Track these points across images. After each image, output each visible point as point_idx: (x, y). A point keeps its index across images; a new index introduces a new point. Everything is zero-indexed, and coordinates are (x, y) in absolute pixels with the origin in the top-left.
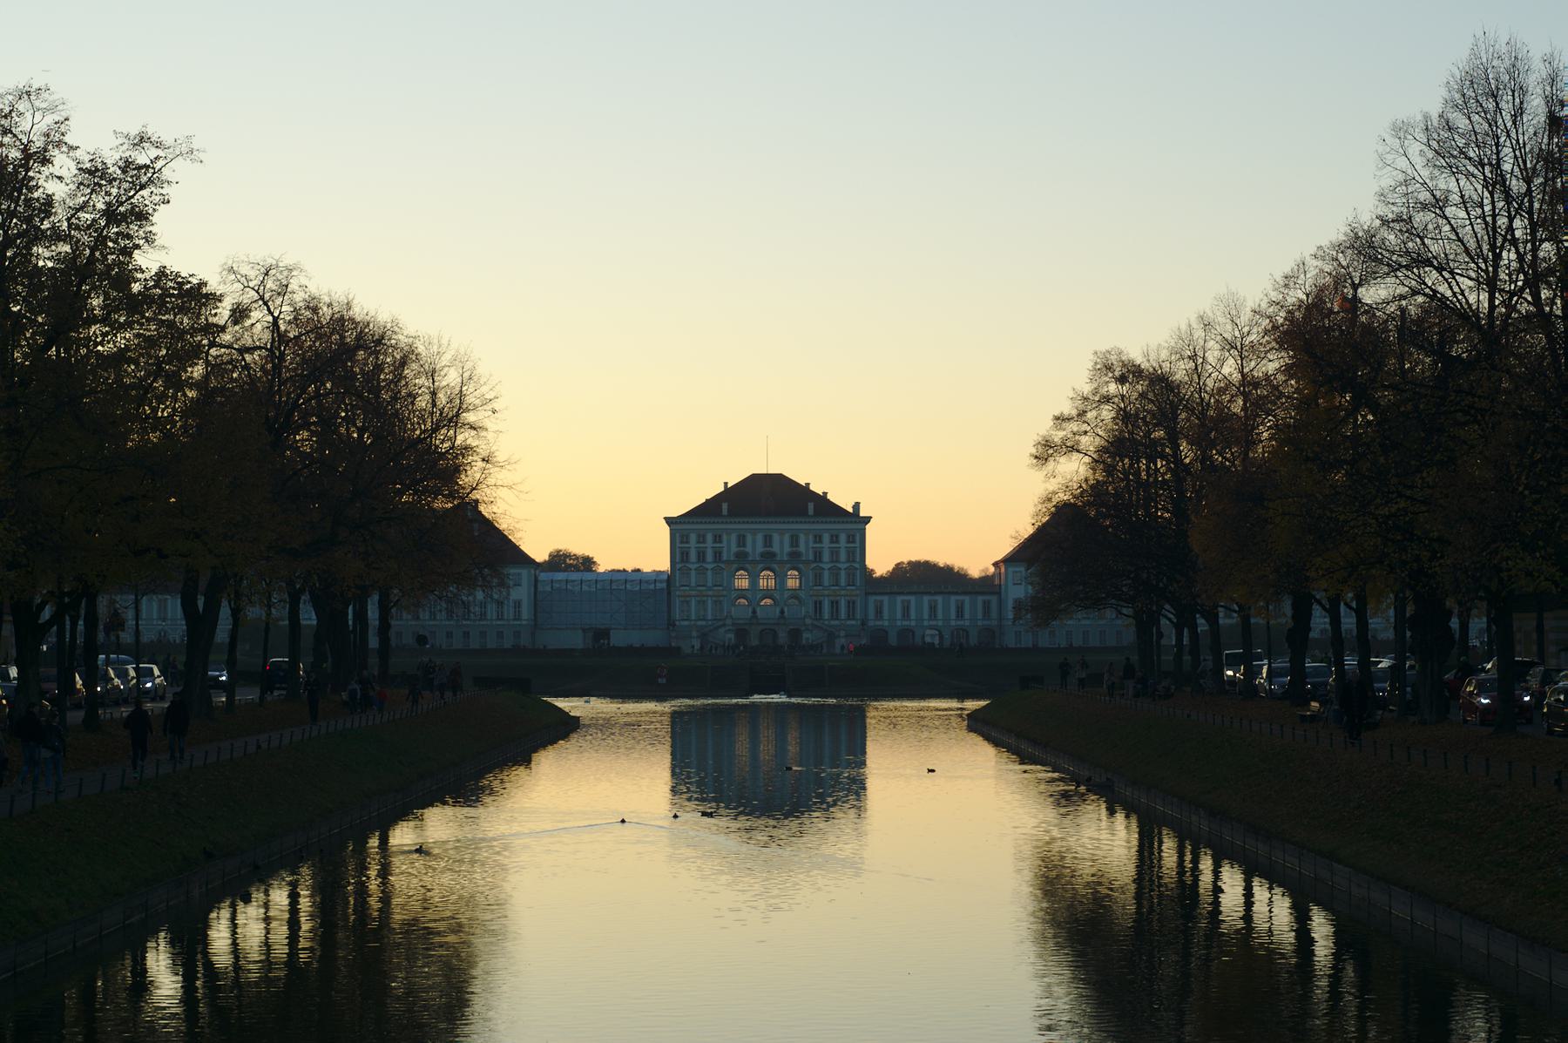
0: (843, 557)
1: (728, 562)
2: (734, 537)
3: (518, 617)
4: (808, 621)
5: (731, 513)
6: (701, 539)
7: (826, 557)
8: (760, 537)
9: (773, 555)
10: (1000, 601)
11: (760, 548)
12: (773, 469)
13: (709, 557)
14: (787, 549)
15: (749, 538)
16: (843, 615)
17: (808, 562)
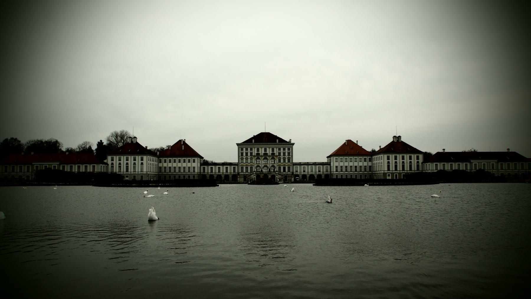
0: (287, 154)
1: (254, 156)
2: (256, 149)
3: (194, 171)
5: (255, 142)
6: (247, 149)
7: (282, 154)
8: (263, 149)
9: (267, 154)
10: (331, 167)
11: (263, 152)
12: (267, 131)
13: (249, 154)
14: (271, 152)
15: (260, 149)
16: (287, 171)
17: (277, 156)
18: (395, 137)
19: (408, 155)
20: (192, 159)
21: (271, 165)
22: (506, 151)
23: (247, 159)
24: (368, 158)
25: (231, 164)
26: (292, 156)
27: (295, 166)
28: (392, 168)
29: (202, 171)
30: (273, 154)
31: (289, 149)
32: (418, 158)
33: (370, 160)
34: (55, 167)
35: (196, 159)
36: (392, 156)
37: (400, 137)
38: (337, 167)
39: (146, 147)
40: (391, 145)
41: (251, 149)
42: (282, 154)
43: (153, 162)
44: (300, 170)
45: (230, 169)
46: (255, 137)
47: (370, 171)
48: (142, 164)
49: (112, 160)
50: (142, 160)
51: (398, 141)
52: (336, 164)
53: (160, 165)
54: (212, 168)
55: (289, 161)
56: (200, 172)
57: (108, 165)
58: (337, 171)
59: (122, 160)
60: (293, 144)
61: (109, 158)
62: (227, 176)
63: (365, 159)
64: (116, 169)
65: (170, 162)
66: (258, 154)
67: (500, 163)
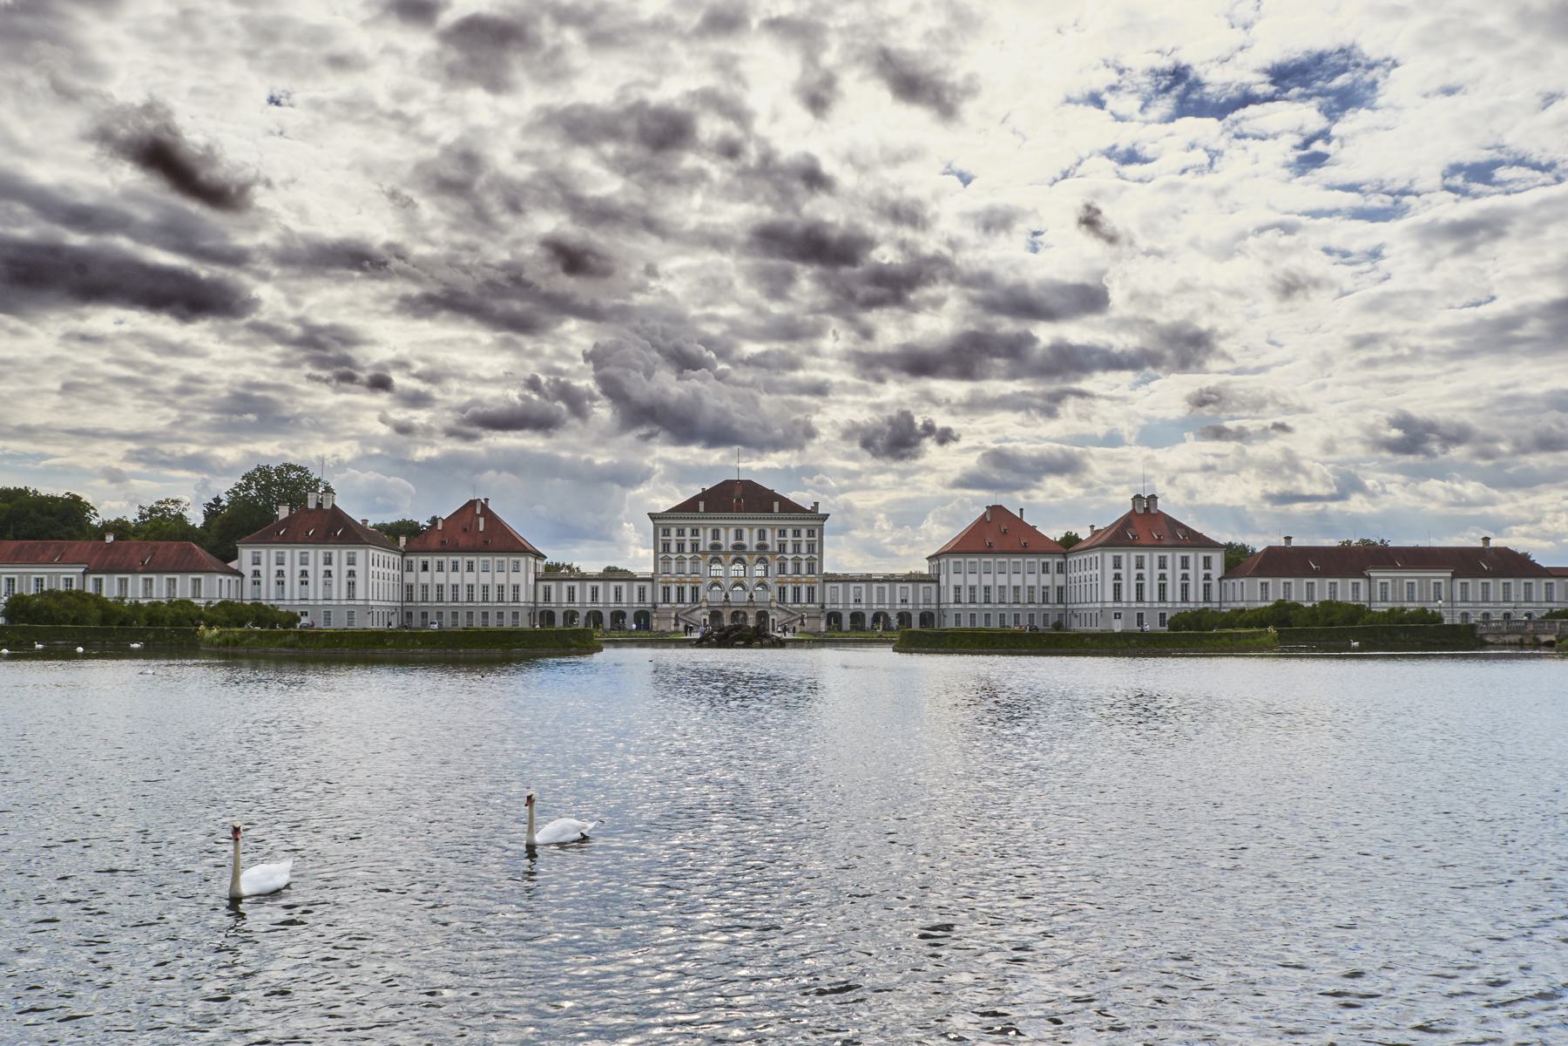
0: (804, 548)
1: (705, 553)
2: (709, 531)
3: (516, 599)
4: (774, 604)
5: (706, 510)
6: (681, 532)
7: (789, 548)
8: (732, 532)
9: (743, 547)
11: (732, 541)
13: (688, 548)
14: (756, 542)
15: (722, 532)
16: (804, 599)
17: (773, 554)
18: (1138, 497)
19: (1179, 555)
20: (508, 560)
21: (755, 581)
22: (1480, 544)
23: (681, 561)
24: (1053, 562)
25: (629, 578)
26: (821, 553)
27: (828, 585)
28: (1128, 593)
29: (541, 598)
30: (762, 547)
31: (811, 533)
32: (1207, 563)
33: (1061, 569)
34: (69, 581)
35: (522, 560)
36: (1129, 557)
37: (1153, 497)
38: (958, 588)
39: (365, 521)
40: (1126, 523)
41: (695, 532)
42: (789, 548)
43: (386, 570)
44: (841, 600)
45: (630, 599)
46: (705, 496)
47: (1060, 601)
48: (351, 573)
49: (257, 562)
50: (351, 562)
51: (1147, 510)
52: (957, 580)
53: (410, 578)
54: (571, 591)
55: (811, 570)
56: (535, 602)
57: (242, 576)
58: (957, 602)
59: (287, 561)
60: (825, 517)
61: (246, 554)
62: (618, 616)
63: (1045, 565)
64: (268, 594)
65: (440, 569)
66: (716, 547)
67: (1459, 581)
